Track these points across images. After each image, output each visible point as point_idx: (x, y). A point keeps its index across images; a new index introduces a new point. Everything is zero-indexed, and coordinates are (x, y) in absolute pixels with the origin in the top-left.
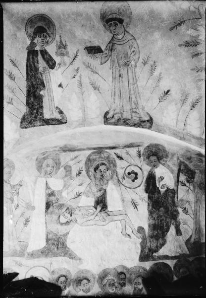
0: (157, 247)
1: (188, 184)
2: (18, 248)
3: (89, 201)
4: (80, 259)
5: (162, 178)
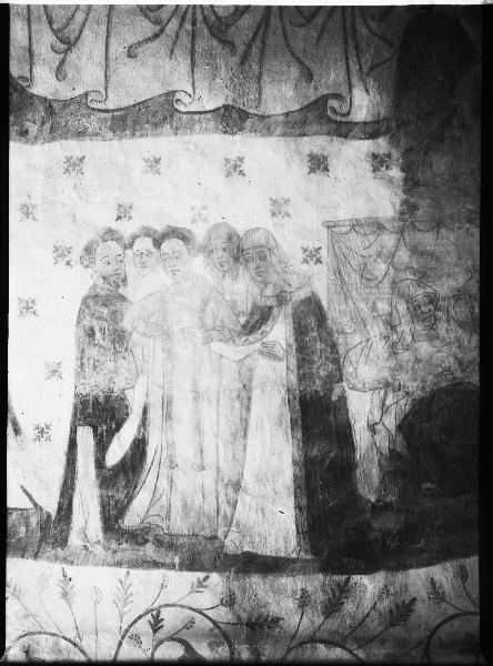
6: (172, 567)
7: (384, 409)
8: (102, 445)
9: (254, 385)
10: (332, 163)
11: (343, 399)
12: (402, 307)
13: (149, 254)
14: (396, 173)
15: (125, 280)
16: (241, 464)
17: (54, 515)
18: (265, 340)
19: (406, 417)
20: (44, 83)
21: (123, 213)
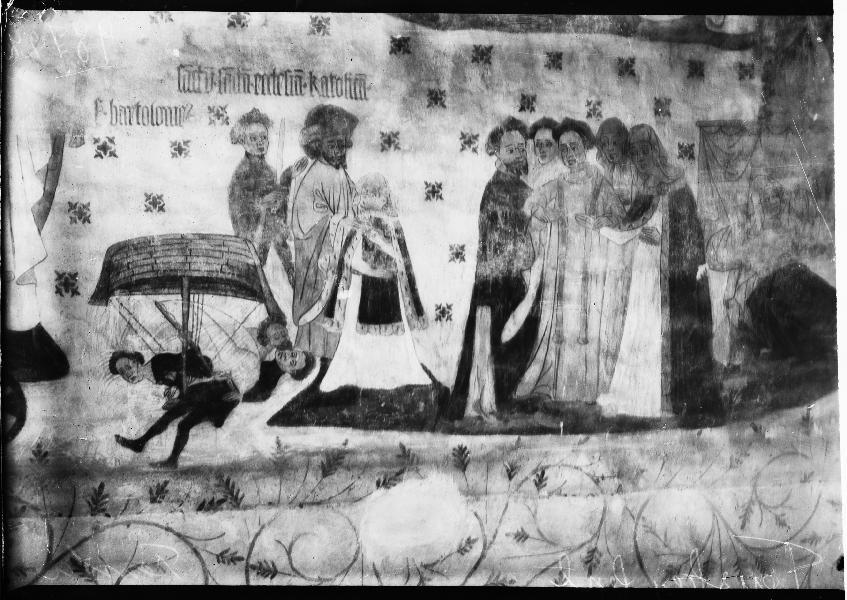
6: (555, 431)
7: (737, 287)
9: (634, 268)
10: (708, 69)
11: (705, 278)
12: (756, 200)
13: (549, 144)
14: (757, 82)
16: (619, 335)
17: (451, 390)
18: (645, 226)
19: (753, 293)
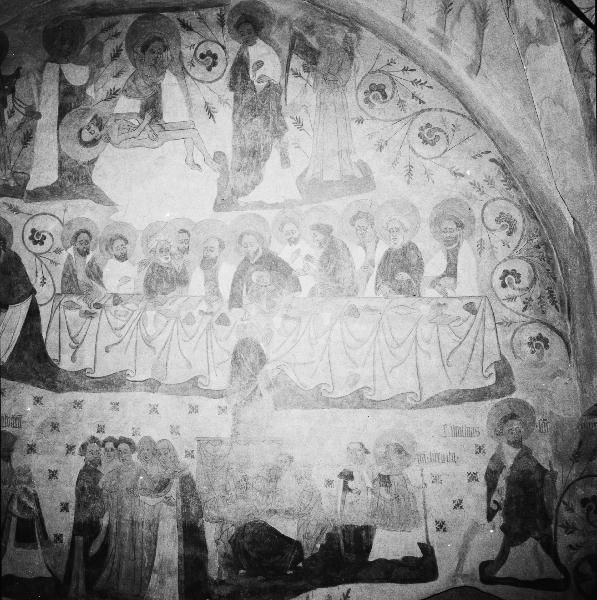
0: (246, 186)
1: (305, 75)
2: (12, 183)
3: (128, 105)
4: (111, 204)
5: (260, 64)
8: (87, 546)
11: (202, 526)
13: (112, 450)
15: (100, 463)
20: (66, 364)
21: (101, 429)
